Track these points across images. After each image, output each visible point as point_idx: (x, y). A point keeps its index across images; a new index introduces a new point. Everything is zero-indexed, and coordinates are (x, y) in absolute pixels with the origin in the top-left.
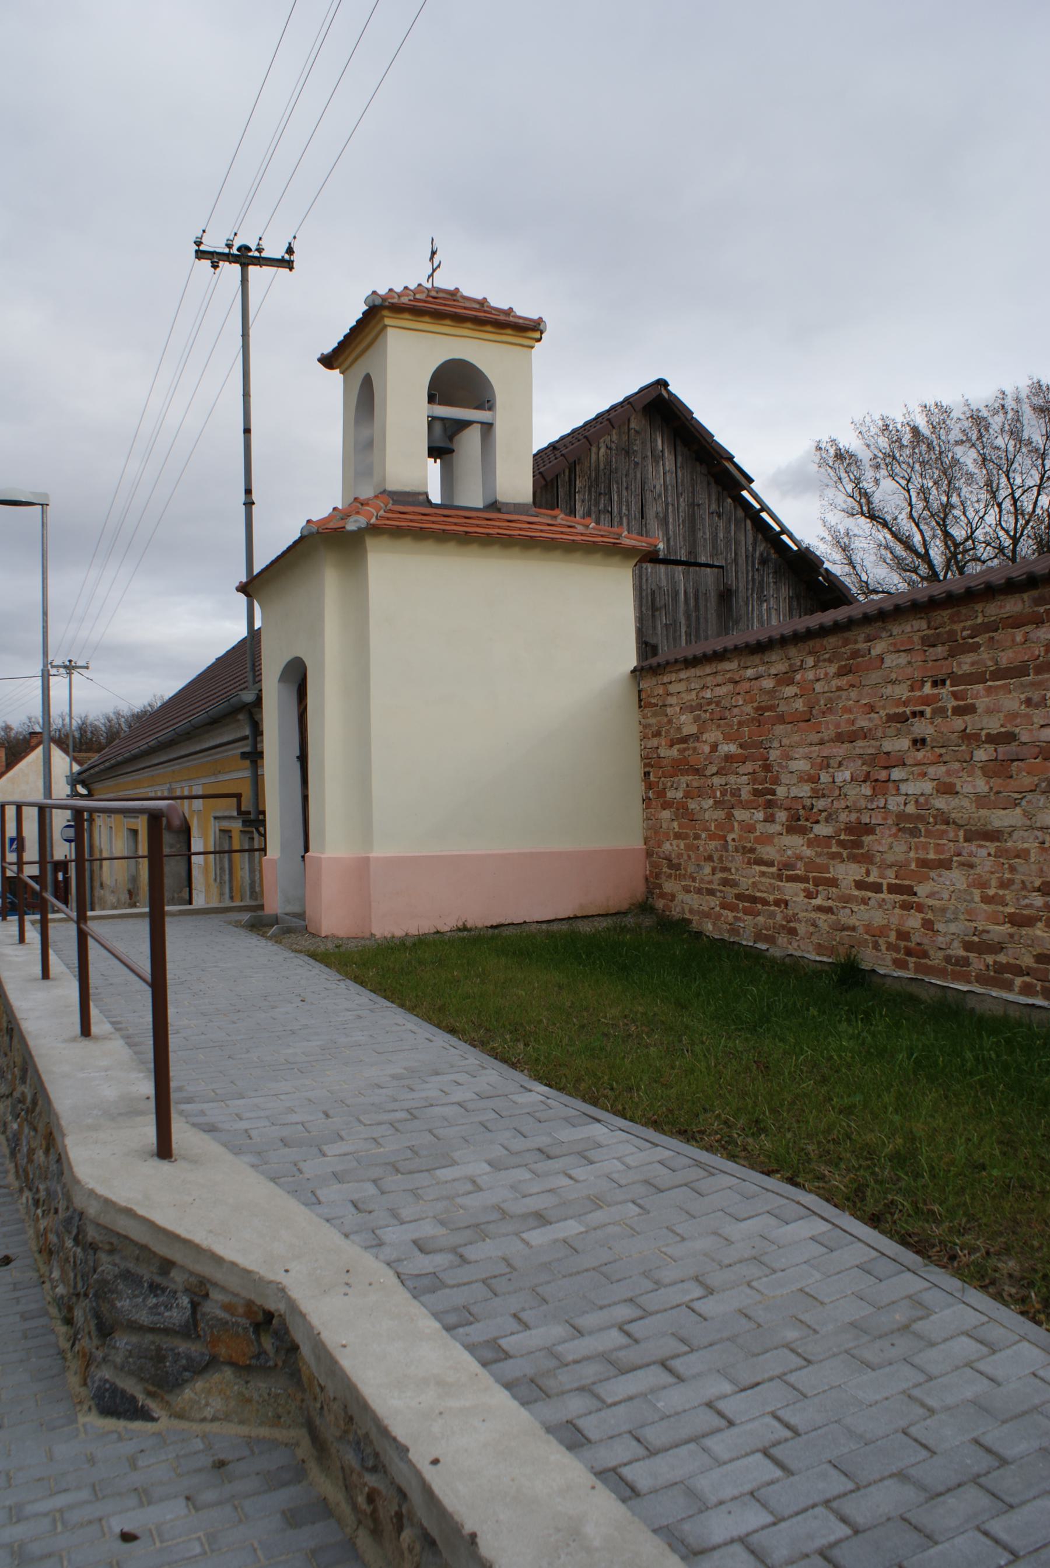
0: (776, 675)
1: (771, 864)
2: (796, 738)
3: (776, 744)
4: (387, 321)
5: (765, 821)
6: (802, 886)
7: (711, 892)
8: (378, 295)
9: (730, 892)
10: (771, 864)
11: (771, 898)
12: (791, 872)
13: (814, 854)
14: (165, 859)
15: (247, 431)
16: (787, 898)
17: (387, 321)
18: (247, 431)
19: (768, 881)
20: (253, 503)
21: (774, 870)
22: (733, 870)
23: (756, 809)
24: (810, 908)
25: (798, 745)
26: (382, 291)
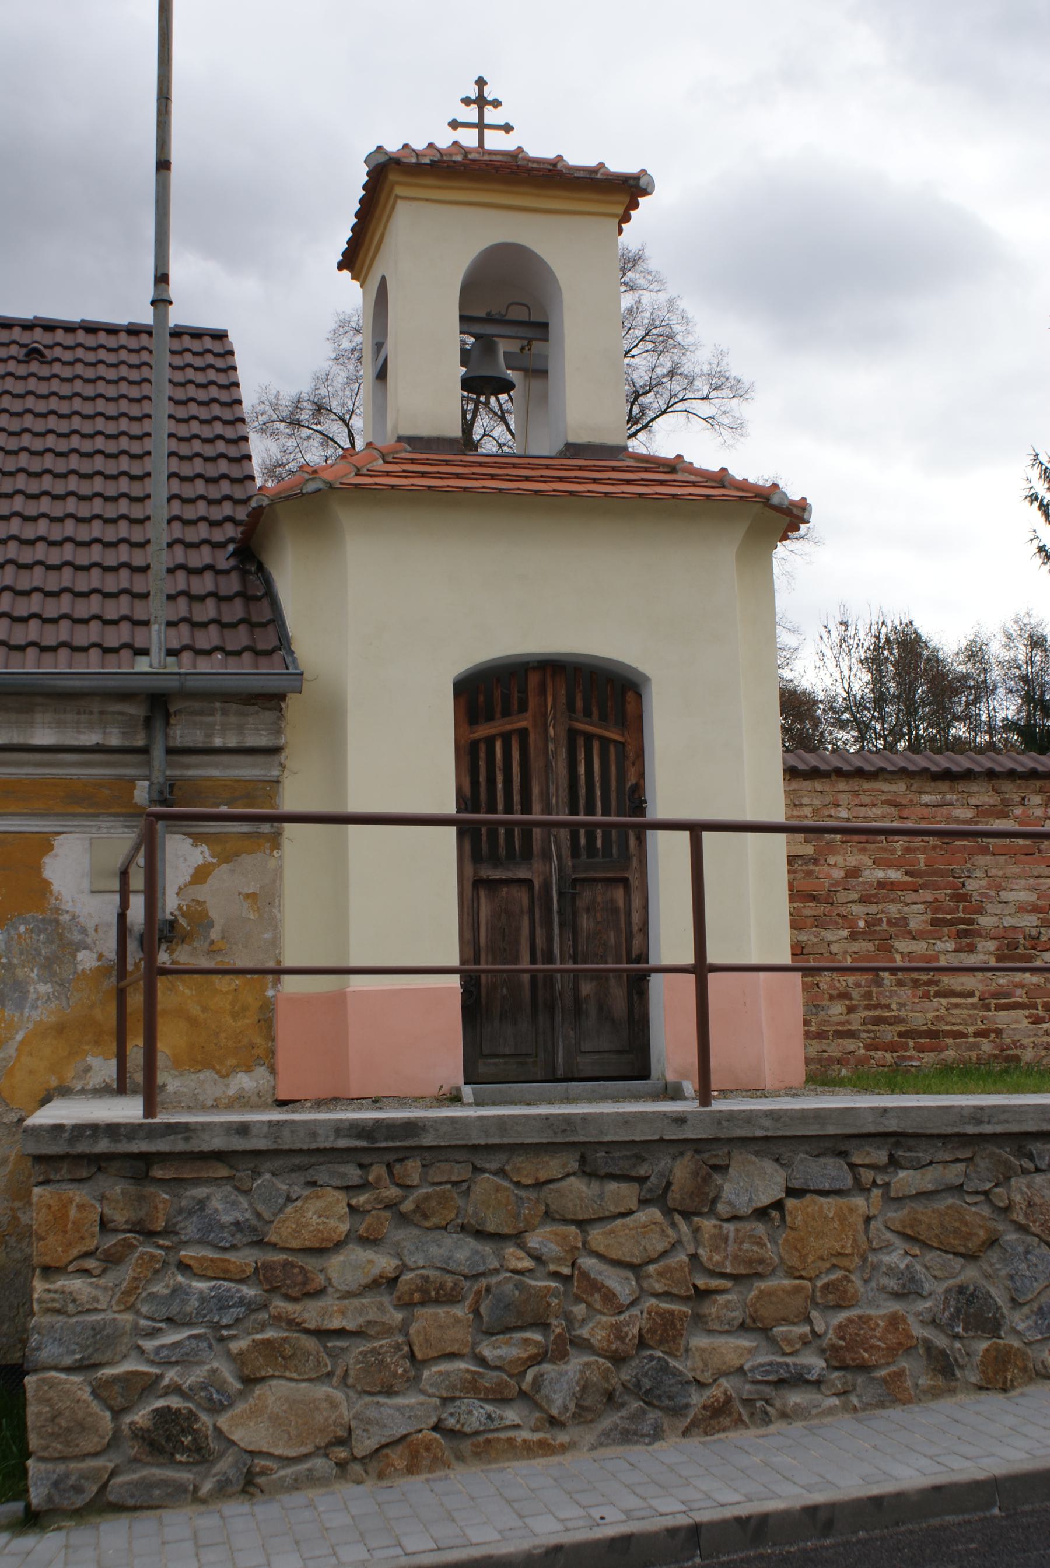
0: (977, 806)
1: (971, 994)
2: (1016, 869)
3: (979, 874)
4: (399, 190)
5: (955, 951)
6: (1027, 1012)
7: (851, 1035)
8: (437, 149)
9: (888, 1033)
10: (971, 994)
11: (971, 1029)
12: (1003, 1001)
13: (1042, 980)
14: (455, 961)
15: (163, 165)
16: (1000, 1026)
17: (399, 190)
18: (163, 165)
19: (965, 1012)
20: (153, 303)
21: (975, 1000)
22: (894, 1006)
23: (940, 939)
24: (1040, 1033)
25: (1017, 877)
26: (393, 147)
